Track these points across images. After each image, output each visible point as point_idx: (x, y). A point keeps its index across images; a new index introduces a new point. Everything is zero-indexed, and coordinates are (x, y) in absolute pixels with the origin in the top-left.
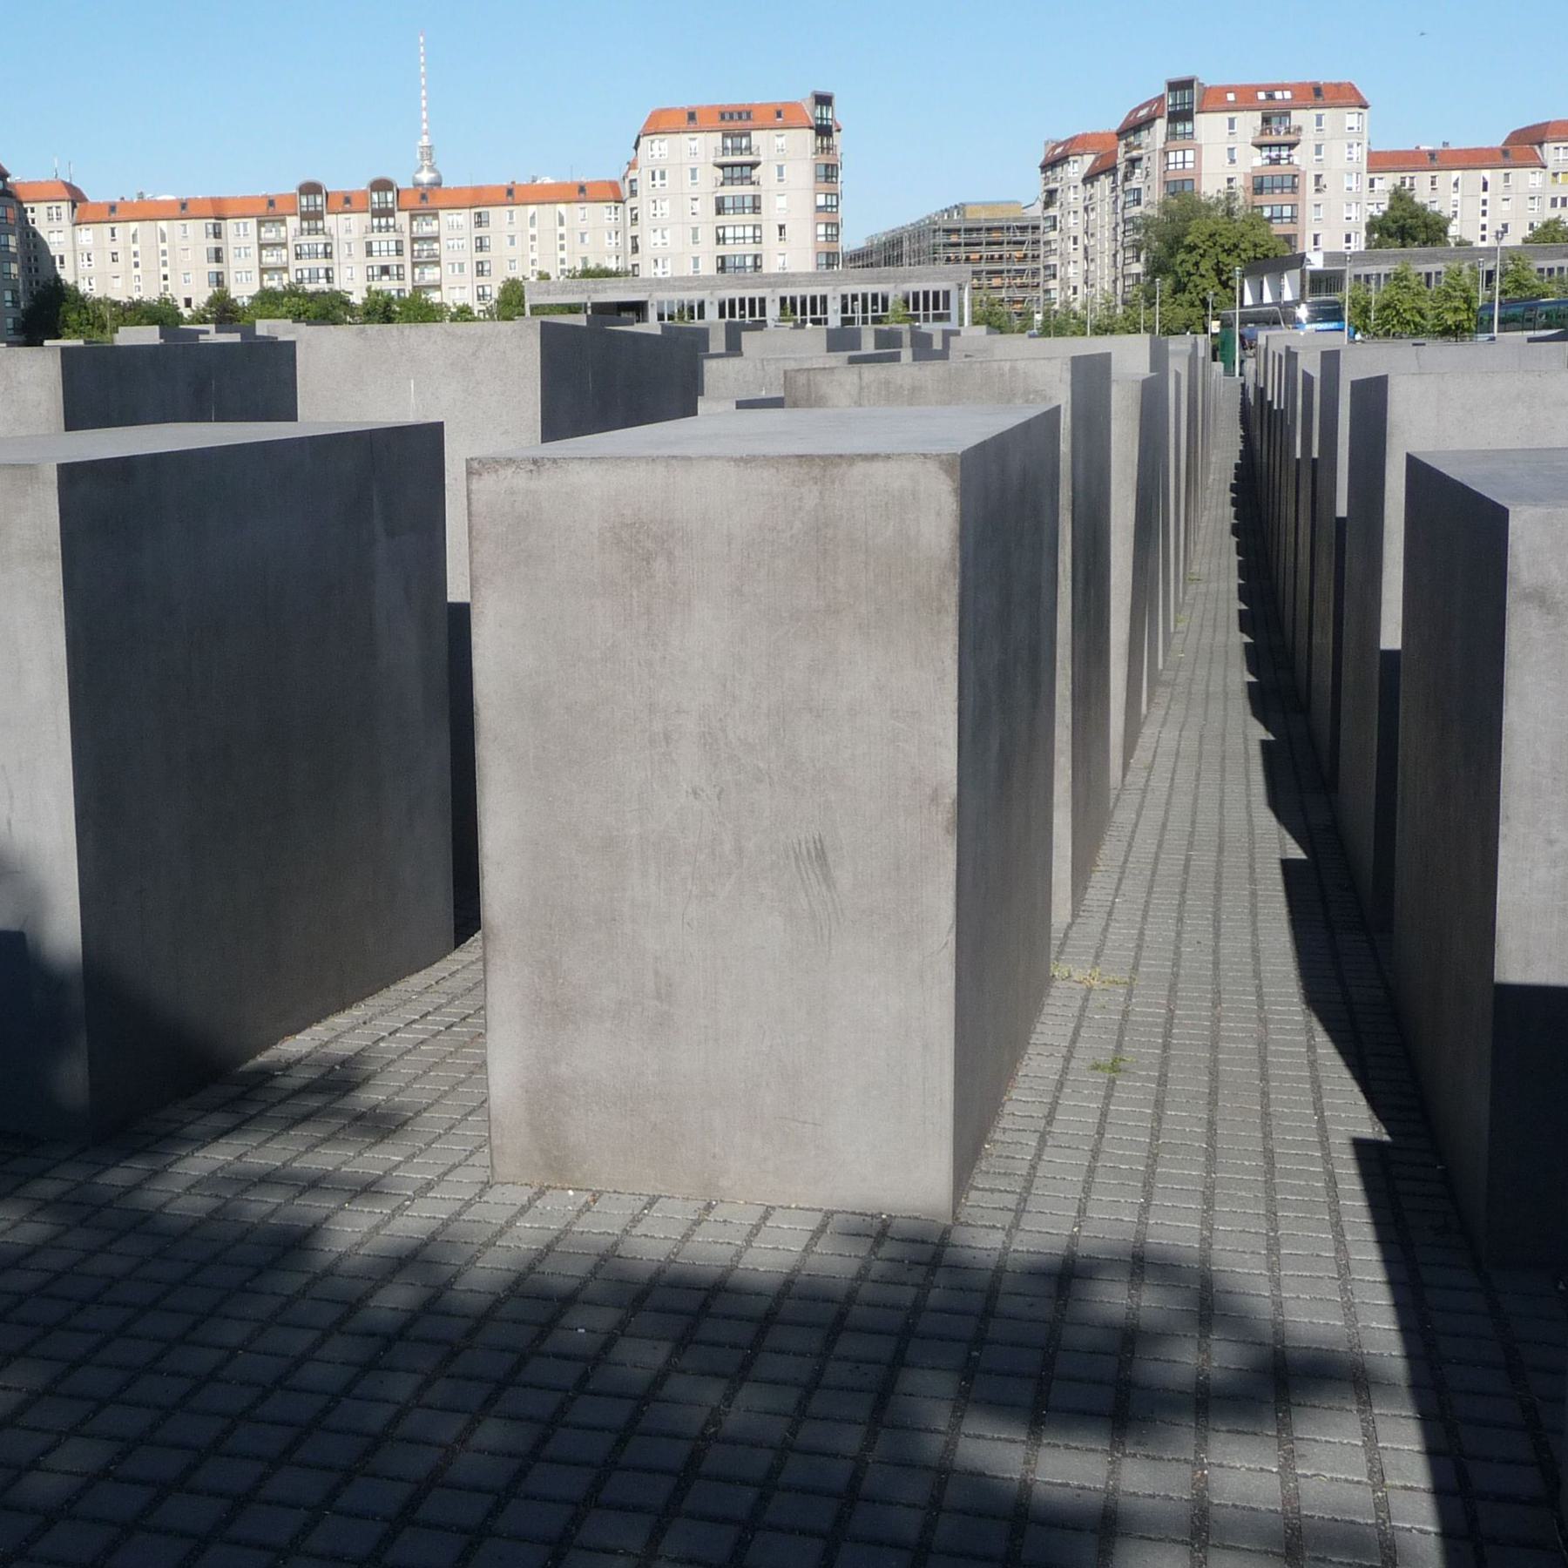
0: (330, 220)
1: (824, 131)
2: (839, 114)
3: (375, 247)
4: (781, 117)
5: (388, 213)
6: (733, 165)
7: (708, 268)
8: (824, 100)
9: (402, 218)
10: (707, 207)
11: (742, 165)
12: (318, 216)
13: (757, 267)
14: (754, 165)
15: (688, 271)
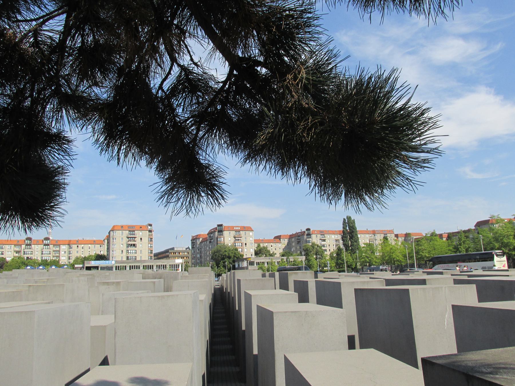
0: (33, 246)
1: (150, 231)
2: (153, 228)
3: (44, 252)
4: (141, 228)
5: (48, 245)
6: (131, 237)
7: (125, 259)
8: (150, 225)
9: (51, 246)
10: (125, 245)
11: (133, 237)
12: (30, 245)
13: (135, 259)
14: (135, 238)
15: (120, 259)
